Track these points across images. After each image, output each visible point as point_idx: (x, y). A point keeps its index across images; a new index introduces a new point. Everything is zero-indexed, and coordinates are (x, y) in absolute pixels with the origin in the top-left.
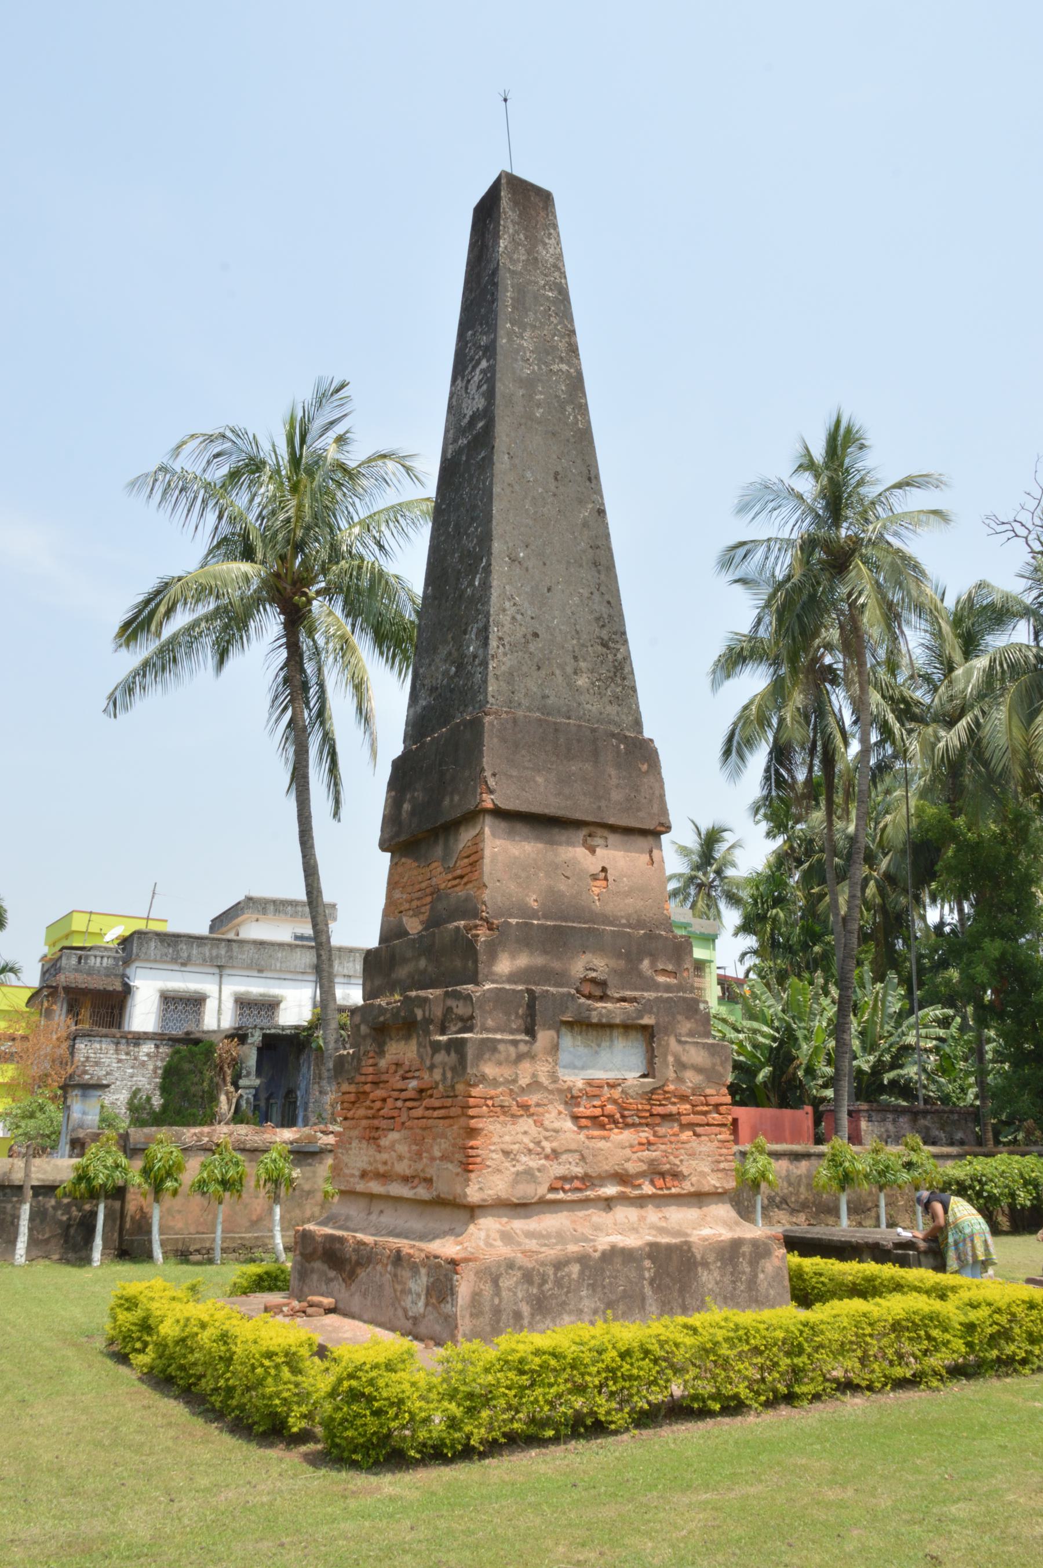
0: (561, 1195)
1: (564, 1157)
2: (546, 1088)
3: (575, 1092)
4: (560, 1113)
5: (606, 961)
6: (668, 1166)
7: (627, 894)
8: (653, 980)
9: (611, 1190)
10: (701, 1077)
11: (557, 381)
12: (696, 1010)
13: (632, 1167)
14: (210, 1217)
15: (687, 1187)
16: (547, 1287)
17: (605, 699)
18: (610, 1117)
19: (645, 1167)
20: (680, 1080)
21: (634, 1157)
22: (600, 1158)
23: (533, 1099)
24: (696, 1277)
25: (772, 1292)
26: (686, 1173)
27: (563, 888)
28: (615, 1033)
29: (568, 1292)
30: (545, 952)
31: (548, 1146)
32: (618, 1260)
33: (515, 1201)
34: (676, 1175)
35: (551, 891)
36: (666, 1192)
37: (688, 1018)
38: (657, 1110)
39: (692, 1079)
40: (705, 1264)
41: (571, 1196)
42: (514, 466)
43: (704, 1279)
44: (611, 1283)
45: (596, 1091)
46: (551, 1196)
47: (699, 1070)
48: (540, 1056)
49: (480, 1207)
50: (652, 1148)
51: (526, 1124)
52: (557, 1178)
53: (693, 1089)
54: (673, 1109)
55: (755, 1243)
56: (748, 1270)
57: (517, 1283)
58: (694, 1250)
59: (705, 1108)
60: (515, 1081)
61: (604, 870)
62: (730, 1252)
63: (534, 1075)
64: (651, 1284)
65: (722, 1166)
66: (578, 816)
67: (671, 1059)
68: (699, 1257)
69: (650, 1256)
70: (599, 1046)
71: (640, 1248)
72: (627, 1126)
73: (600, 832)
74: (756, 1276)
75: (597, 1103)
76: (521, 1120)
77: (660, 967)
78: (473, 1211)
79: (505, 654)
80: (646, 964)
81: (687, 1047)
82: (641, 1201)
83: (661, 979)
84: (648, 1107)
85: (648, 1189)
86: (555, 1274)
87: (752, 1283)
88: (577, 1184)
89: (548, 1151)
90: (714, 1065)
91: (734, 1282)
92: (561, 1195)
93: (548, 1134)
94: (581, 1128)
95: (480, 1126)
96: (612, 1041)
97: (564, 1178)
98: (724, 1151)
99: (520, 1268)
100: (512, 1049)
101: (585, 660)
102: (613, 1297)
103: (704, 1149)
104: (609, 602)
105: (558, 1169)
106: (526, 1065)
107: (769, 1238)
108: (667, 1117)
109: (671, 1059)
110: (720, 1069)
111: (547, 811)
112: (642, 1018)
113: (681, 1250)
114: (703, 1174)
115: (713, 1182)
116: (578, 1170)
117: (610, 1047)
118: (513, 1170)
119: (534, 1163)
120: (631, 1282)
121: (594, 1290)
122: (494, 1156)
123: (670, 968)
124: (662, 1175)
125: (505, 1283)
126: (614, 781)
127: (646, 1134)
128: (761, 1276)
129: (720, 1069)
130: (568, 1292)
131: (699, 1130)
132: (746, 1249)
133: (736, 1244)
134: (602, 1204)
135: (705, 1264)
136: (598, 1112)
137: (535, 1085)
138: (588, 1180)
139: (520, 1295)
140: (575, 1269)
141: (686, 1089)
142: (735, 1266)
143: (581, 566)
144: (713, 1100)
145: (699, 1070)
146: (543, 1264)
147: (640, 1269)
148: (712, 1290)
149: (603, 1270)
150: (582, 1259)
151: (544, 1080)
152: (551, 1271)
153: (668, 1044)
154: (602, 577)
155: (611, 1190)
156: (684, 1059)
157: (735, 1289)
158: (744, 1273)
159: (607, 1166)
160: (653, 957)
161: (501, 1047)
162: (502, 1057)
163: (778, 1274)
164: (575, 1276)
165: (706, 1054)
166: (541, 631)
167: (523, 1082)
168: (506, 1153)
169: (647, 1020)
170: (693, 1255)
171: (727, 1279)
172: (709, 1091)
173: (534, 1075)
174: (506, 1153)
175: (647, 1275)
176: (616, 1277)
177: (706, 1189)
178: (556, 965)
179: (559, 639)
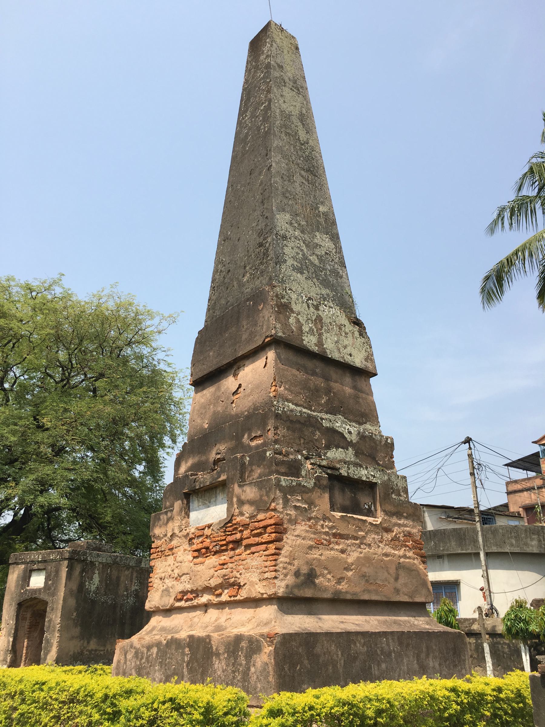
0: (182, 604)
1: (183, 578)
2: (178, 536)
3: (191, 536)
4: (185, 550)
5: (226, 445)
6: (233, 580)
7: (249, 396)
8: (249, 445)
9: (204, 599)
10: (253, 508)
11: (259, 119)
12: (264, 457)
13: (213, 583)
14: (359, 638)
15: (243, 594)
16: (143, 661)
17: (256, 279)
18: (207, 548)
19: (220, 581)
20: (241, 514)
21: (216, 573)
22: (198, 577)
23: (174, 543)
24: (212, 665)
25: (259, 686)
26: (242, 584)
27: (219, 409)
28: (218, 492)
29: (151, 666)
30: (199, 453)
31: (176, 571)
32: (173, 647)
33: (161, 608)
34: (240, 587)
35: (214, 413)
36: (232, 599)
37: (259, 466)
38: (230, 538)
39: (248, 509)
40: (218, 655)
41: (188, 604)
42: (232, 190)
43: (216, 666)
44: (169, 662)
45: (200, 533)
46: (178, 604)
47: (251, 503)
48: (175, 517)
49: (153, 612)
50: (225, 567)
51: (170, 559)
52: (180, 592)
53: (251, 517)
54: (238, 536)
55: (251, 640)
56: (244, 662)
57: (133, 657)
58: (213, 643)
59: (258, 531)
60: (166, 535)
61: (240, 386)
62: (235, 645)
63: (173, 530)
64: (187, 666)
65: (266, 575)
66: (225, 362)
67: (235, 500)
68: (214, 648)
69: (189, 645)
70: (210, 502)
71: (185, 640)
72: (216, 553)
73: (241, 363)
74: (249, 669)
75: (201, 539)
76: (169, 558)
77: (254, 435)
78: (149, 615)
79: (214, 294)
80: (246, 436)
81: (245, 488)
82: (221, 605)
83: (253, 444)
84: (224, 537)
85: (225, 597)
86: (147, 653)
87: (246, 674)
88: (190, 596)
89: (176, 575)
90: (261, 496)
91: (234, 672)
92: (182, 604)
93: (177, 565)
94: (194, 557)
95: (153, 564)
96: (216, 497)
97: (184, 593)
98: (268, 563)
99: (135, 648)
100: (165, 517)
101: (249, 264)
102: (169, 673)
103: (255, 563)
104: (267, 218)
105: (180, 587)
106: (170, 524)
107: (262, 635)
108: (237, 543)
109: (235, 500)
110: (265, 498)
111: (211, 370)
112: (220, 477)
113: (205, 642)
114: (253, 584)
115: (259, 589)
116: (188, 587)
117: (215, 501)
118: (162, 588)
119: (169, 582)
120: (178, 663)
121: (161, 667)
122: (156, 581)
123: (259, 433)
124: (233, 585)
125: (129, 656)
126: (245, 327)
127: (224, 557)
128: (253, 669)
129: (265, 498)
130: (151, 666)
131: (253, 549)
132: (244, 644)
133: (239, 638)
134: (204, 608)
135: (218, 655)
136: (200, 546)
137: (173, 535)
138: (196, 593)
139: (133, 664)
140: (155, 650)
141: (244, 519)
142: (236, 659)
143: (255, 211)
144: (262, 524)
145: (251, 503)
146: (143, 647)
147: (183, 654)
148: (219, 676)
149: (166, 653)
150: (158, 644)
151: (177, 531)
152: (145, 650)
153: (233, 490)
154: (265, 206)
155: (204, 599)
156: (243, 497)
157: (234, 678)
158: (241, 665)
159: (200, 583)
160: (250, 430)
161: (161, 517)
162: (161, 522)
163: (265, 669)
164: (154, 656)
165: (257, 490)
166: (232, 267)
167: (169, 535)
168: (161, 579)
169: (223, 477)
170: (212, 647)
171: (230, 668)
172: (261, 516)
173: (173, 530)
174: (161, 579)
175: (186, 660)
176: (171, 659)
177: (254, 595)
178: (203, 458)
179: (239, 263)
